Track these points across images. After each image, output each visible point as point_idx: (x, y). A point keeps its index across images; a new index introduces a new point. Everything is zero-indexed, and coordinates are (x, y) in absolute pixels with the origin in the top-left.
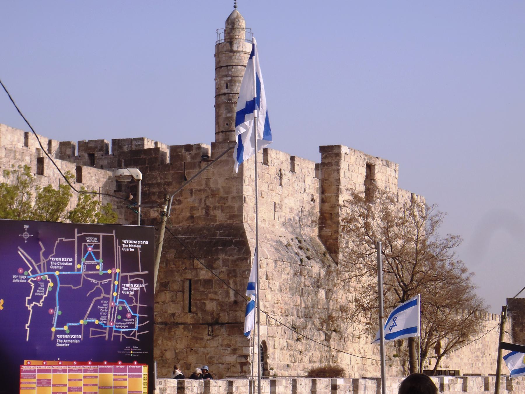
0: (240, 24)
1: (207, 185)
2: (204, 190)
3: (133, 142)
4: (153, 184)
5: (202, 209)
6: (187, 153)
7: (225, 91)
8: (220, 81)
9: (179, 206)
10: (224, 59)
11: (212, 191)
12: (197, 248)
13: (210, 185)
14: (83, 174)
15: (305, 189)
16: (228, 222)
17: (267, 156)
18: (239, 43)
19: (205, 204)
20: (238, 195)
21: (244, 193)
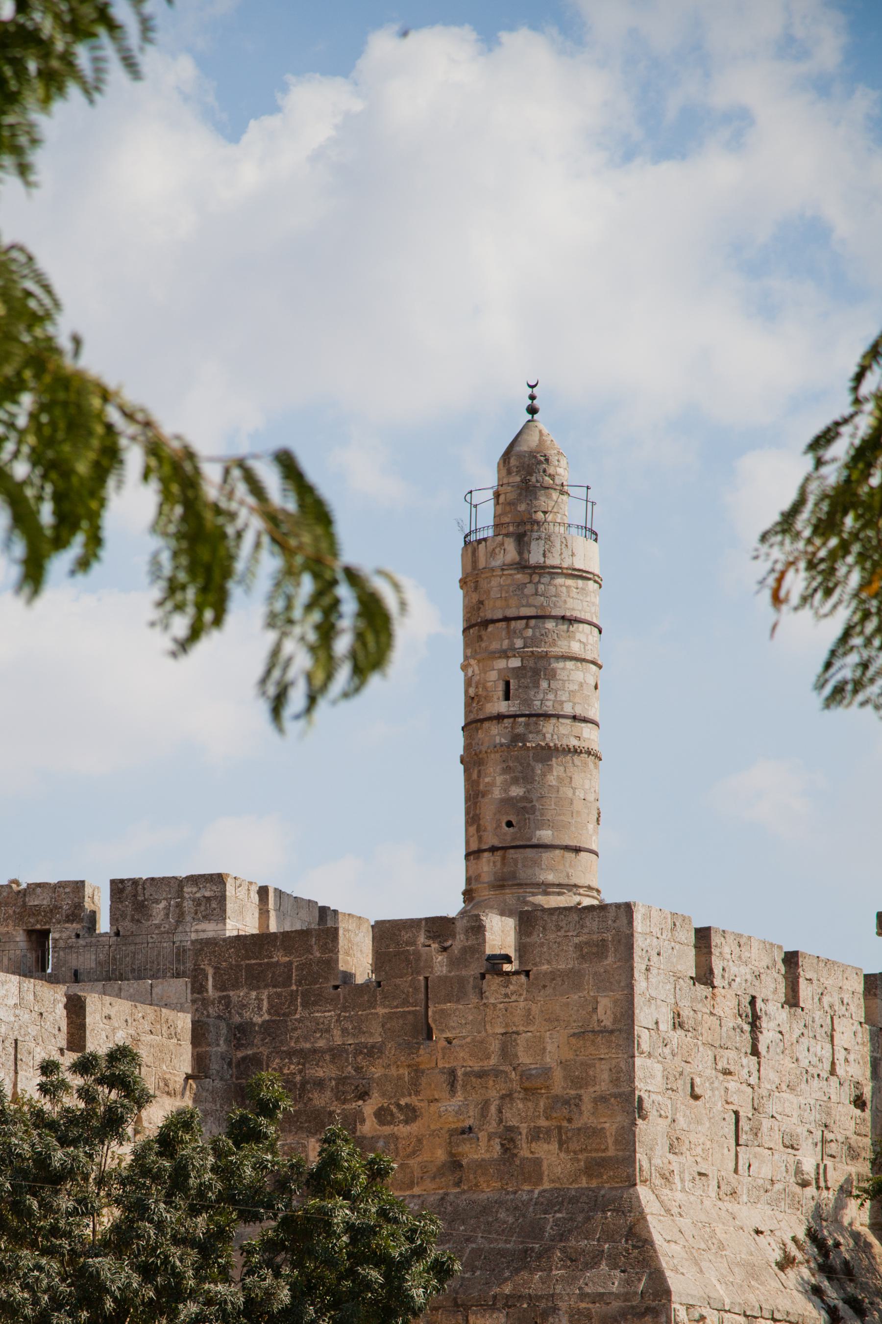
0: (551, 470)
1: (506, 1053)
2: (497, 1073)
3: (185, 889)
4: (314, 1051)
5: (490, 1138)
6: (433, 946)
7: (502, 707)
8: (484, 671)
9: (408, 1128)
10: (495, 593)
11: (525, 1075)
12: (478, 1273)
13: (516, 1056)
14: (88, 1020)
15: (833, 1064)
16: (584, 1183)
17: (710, 953)
18: (548, 538)
19: (501, 1121)
20: (615, 1090)
21: (637, 1083)
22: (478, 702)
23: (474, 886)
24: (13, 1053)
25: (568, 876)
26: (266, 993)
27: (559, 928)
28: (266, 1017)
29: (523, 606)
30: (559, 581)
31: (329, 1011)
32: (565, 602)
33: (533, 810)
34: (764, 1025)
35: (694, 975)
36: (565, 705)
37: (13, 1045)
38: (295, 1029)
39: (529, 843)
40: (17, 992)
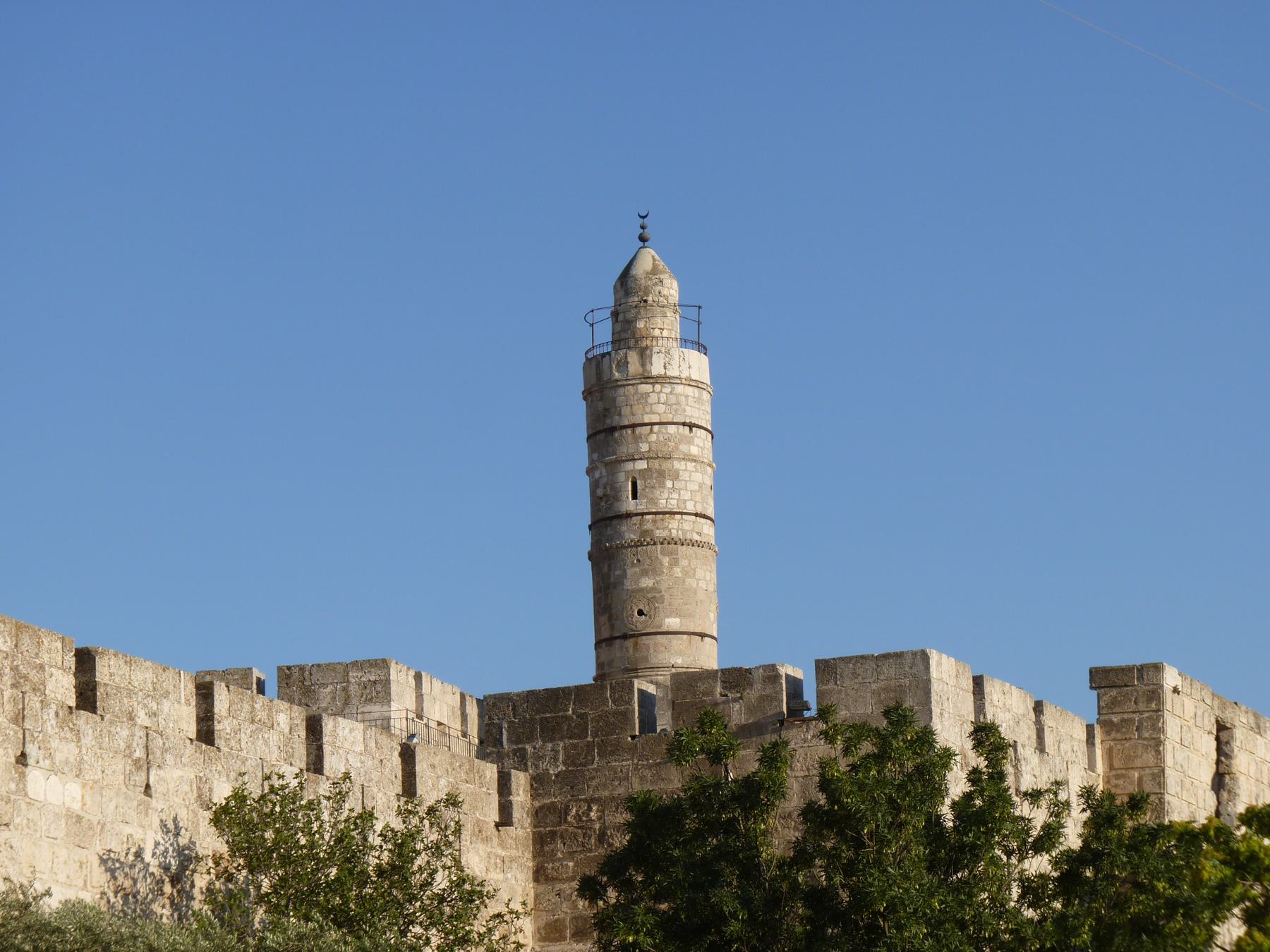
0: (665, 292)
3: (351, 674)
14: (418, 768)
22: (606, 502)
23: (606, 670)
24: (361, 798)
25: (694, 660)
26: (561, 744)
27: (855, 675)
28: (562, 768)
29: (647, 413)
30: (679, 389)
31: (626, 760)
32: (685, 411)
33: (662, 600)
34: (1024, 768)
35: (974, 721)
36: (688, 503)
37: (361, 791)
38: (593, 778)
39: (659, 630)
40: (362, 739)
